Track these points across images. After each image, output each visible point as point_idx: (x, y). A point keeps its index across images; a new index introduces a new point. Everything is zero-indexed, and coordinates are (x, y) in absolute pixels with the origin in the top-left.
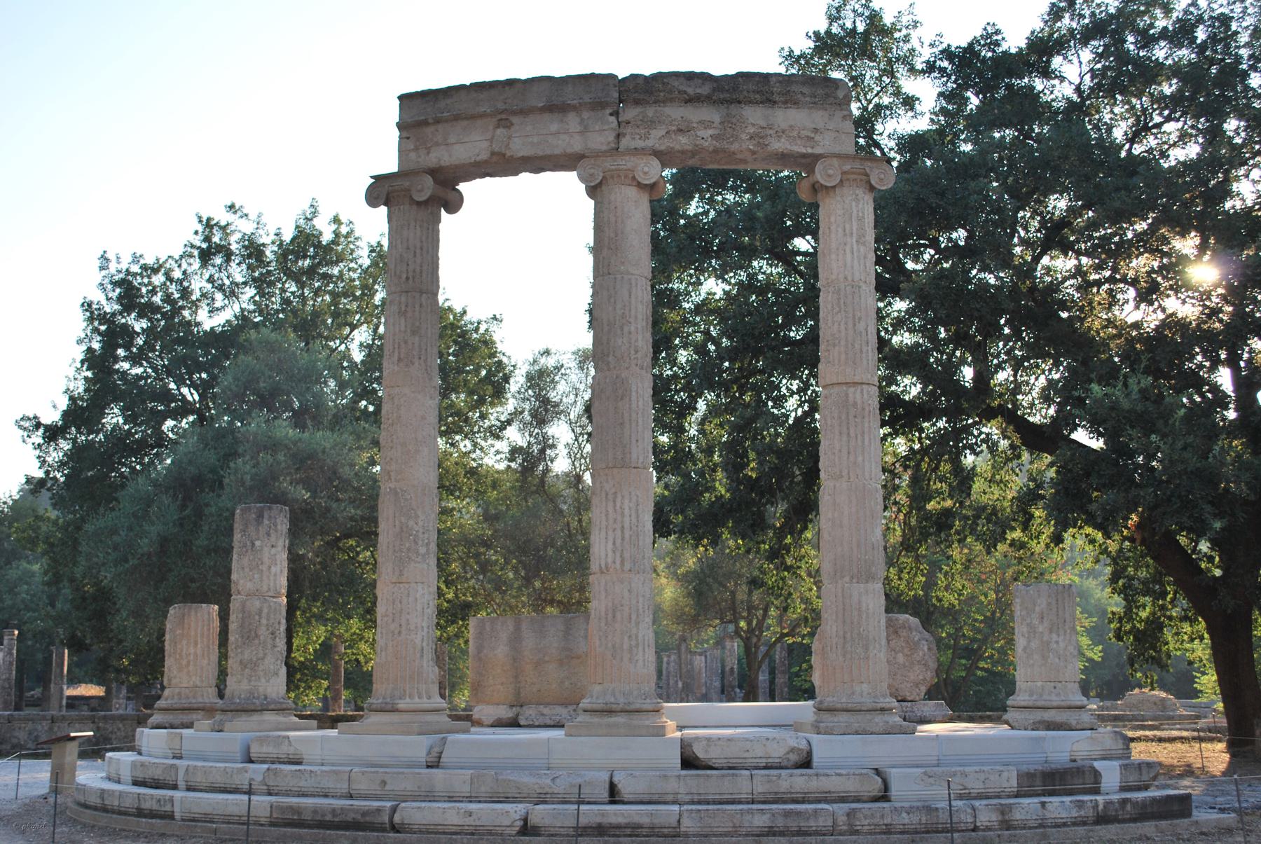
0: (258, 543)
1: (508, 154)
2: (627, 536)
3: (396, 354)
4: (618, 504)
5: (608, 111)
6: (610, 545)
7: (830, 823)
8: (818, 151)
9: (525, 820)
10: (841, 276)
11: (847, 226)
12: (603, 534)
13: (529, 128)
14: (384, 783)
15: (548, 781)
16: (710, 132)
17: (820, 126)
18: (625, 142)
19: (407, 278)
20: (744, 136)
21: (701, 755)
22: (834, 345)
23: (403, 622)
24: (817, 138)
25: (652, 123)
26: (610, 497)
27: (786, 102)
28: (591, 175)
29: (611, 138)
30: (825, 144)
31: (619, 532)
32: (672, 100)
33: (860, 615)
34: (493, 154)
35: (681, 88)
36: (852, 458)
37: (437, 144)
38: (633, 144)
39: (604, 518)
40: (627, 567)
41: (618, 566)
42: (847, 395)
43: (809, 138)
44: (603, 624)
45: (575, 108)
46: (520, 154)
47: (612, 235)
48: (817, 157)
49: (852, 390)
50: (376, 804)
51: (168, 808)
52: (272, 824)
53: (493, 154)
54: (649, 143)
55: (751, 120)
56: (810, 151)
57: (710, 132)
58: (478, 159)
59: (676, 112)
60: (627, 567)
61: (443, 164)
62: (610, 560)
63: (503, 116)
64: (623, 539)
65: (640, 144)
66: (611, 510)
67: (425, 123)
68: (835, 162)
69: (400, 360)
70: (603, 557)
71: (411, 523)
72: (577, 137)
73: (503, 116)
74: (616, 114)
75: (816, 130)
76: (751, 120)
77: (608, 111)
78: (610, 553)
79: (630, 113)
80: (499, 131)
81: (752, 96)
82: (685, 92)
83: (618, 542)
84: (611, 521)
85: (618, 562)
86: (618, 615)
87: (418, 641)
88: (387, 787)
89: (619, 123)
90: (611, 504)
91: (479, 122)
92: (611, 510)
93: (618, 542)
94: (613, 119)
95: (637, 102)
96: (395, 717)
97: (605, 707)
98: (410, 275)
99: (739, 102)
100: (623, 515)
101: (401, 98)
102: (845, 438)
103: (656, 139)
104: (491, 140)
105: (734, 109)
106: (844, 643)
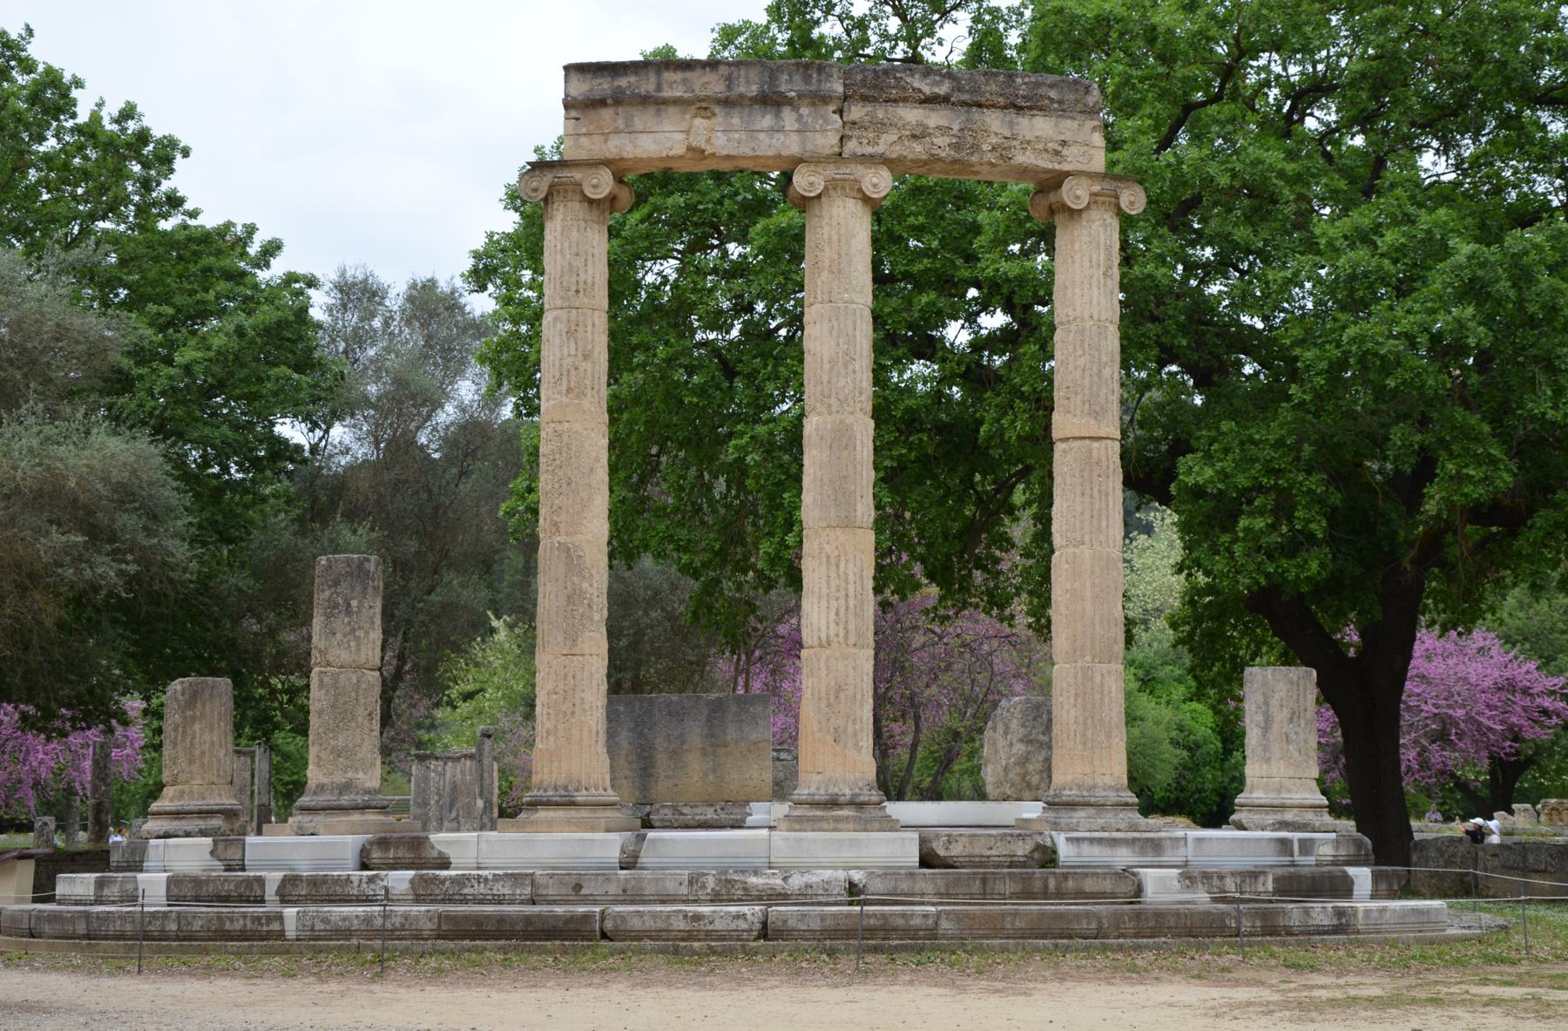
0: (354, 603)
1: (709, 150)
2: (851, 604)
3: (565, 382)
4: (842, 569)
5: (832, 108)
6: (832, 615)
7: (1094, 926)
8: (1066, 167)
9: (765, 924)
10: (1086, 315)
11: (1094, 257)
12: (824, 604)
13: (736, 121)
14: (578, 887)
15: (779, 881)
16: (947, 140)
17: (1067, 136)
18: (851, 146)
19: (577, 291)
20: (985, 147)
21: (942, 853)
22: (1076, 393)
23: (577, 701)
24: (1065, 152)
25: (881, 127)
26: (832, 560)
27: (1031, 108)
28: (811, 184)
29: (835, 140)
30: (1072, 160)
31: (842, 601)
32: (905, 100)
33: (1102, 699)
34: (690, 148)
35: (916, 85)
36: (1095, 522)
37: (617, 131)
38: (859, 151)
39: (824, 585)
40: (852, 640)
41: (841, 639)
42: (1090, 451)
43: (1057, 153)
44: (823, 705)
45: (790, 102)
46: (724, 153)
47: (835, 257)
48: (1068, 174)
49: (1096, 445)
50: (581, 909)
51: (275, 926)
52: (439, 937)
53: (690, 148)
54: (879, 149)
55: (994, 128)
56: (1057, 167)
57: (947, 140)
58: (672, 153)
59: (911, 115)
60: (852, 640)
61: (625, 155)
62: (832, 633)
64: (847, 608)
65: (869, 150)
66: (833, 575)
67: (601, 103)
68: (1084, 181)
69: (569, 390)
70: (823, 628)
71: (585, 585)
72: (795, 137)
74: (840, 112)
75: (1064, 143)
76: (994, 128)
77: (832, 108)
78: (832, 625)
79: (856, 112)
81: (995, 98)
82: (920, 91)
83: (842, 612)
84: (833, 588)
85: (842, 633)
86: (842, 695)
87: (593, 723)
88: (583, 892)
89: (844, 123)
90: (833, 568)
91: (672, 110)
92: (833, 575)
93: (842, 612)
94: (836, 117)
95: (865, 99)
96: (572, 813)
97: (809, 799)
98: (581, 287)
99: (980, 106)
100: (846, 580)
101: (567, 68)
102: (1087, 497)
103: (886, 144)
104: (687, 132)
105: (975, 113)
106: (1086, 729)
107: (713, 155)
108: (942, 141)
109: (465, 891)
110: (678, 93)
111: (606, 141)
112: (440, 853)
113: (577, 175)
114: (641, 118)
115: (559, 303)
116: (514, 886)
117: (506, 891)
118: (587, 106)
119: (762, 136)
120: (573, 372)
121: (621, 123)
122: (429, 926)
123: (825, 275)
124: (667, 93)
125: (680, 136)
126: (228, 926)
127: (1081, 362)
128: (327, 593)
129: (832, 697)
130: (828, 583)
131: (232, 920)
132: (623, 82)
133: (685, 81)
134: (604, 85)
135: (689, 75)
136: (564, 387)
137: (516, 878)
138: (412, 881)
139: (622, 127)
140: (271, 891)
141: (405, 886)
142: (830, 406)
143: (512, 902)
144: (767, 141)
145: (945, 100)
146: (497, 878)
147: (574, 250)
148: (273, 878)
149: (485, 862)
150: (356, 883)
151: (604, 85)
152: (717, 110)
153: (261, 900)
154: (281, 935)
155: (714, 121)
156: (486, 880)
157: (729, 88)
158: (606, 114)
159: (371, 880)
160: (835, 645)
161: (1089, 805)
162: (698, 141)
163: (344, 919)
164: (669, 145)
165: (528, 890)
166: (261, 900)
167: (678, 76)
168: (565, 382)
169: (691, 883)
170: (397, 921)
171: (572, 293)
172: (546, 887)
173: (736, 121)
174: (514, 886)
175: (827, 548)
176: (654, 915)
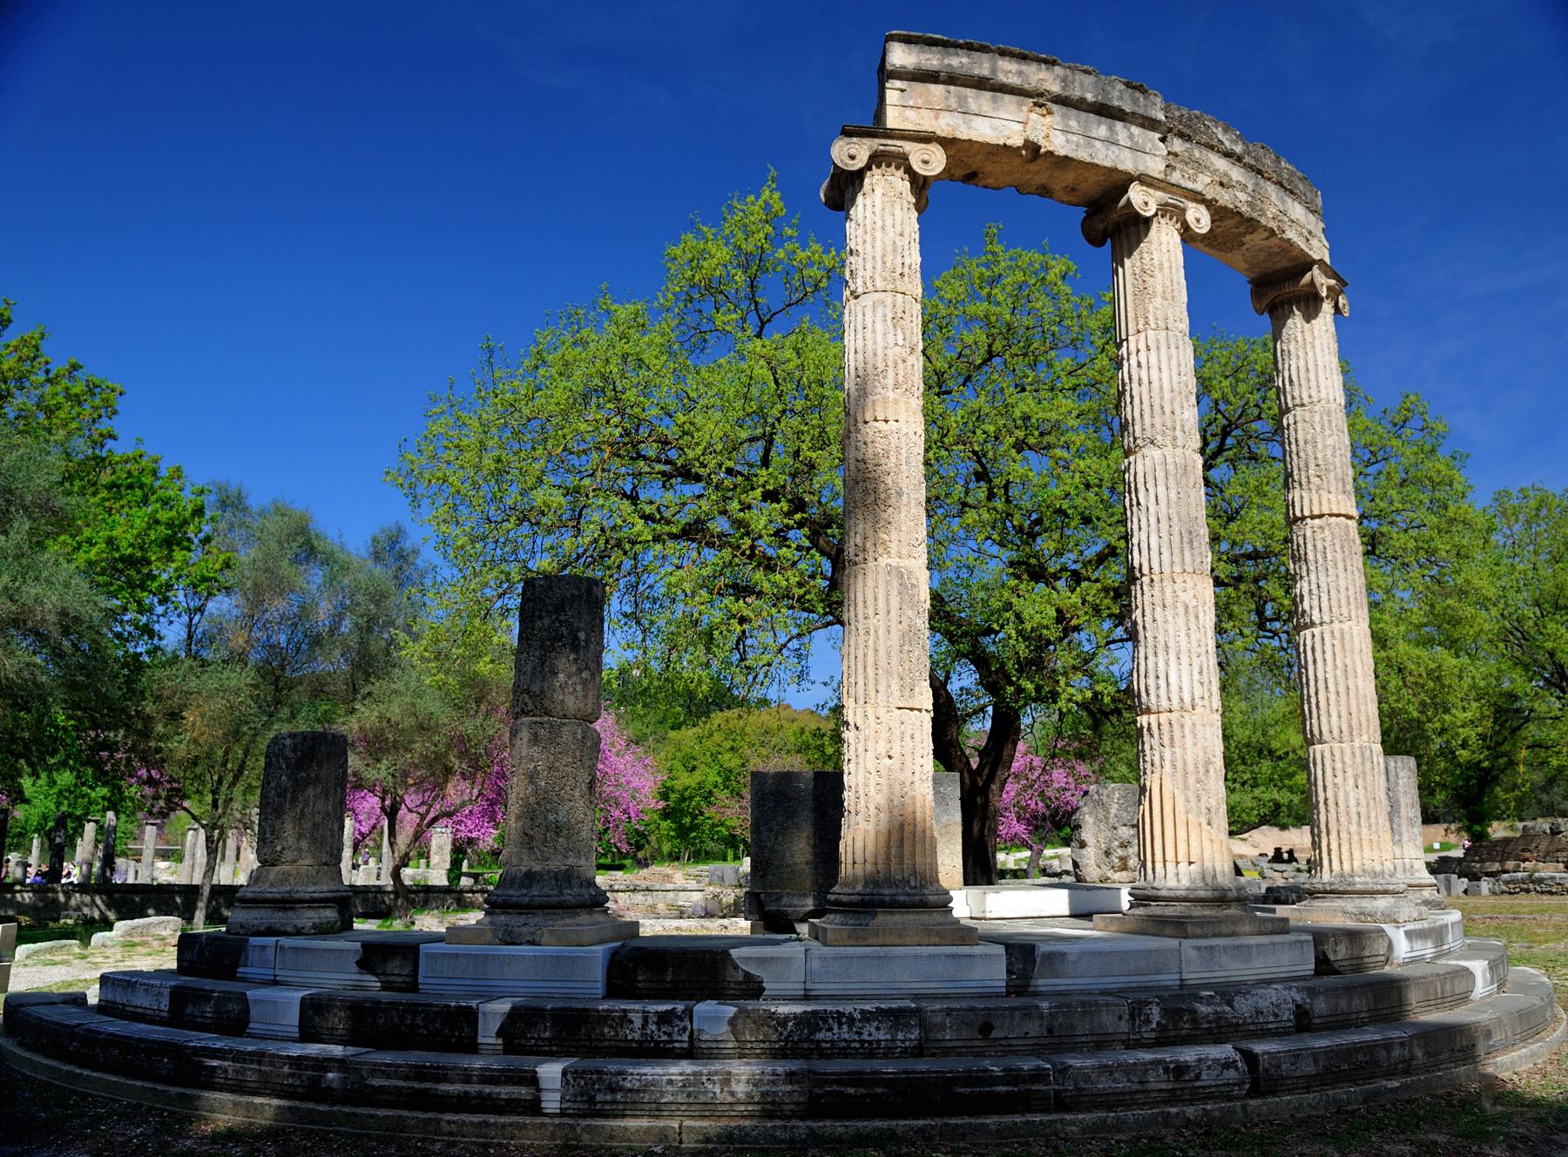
0: (582, 635)
14: (986, 1029)
25: (1199, 166)
31: (1203, 658)
34: (1027, 141)
39: (1183, 638)
47: (1168, 283)
54: (1198, 187)
58: (1009, 143)
59: (1221, 164)
61: (959, 136)
63: (1041, 101)
65: (1190, 185)
69: (896, 386)
73: (1041, 101)
79: (1178, 145)
80: (1033, 116)
84: (1194, 644)
88: (994, 1034)
90: (1192, 619)
107: (1050, 153)
108: (1242, 196)
109: (820, 1036)
110: (1013, 80)
111: (936, 118)
112: (747, 974)
113: (907, 146)
114: (979, 100)
115: (880, 285)
116: (895, 1027)
117: (882, 1035)
118: (914, 79)
119: (1098, 144)
120: (901, 366)
121: (953, 102)
123: (1158, 301)
124: (1002, 78)
125: (1019, 127)
127: (1330, 441)
128: (547, 621)
129: (1202, 770)
130: (1188, 635)
133: (1020, 73)
135: (1024, 67)
137: (896, 1017)
139: (954, 106)
142: (1175, 438)
143: (888, 1054)
144: (1103, 150)
145: (1239, 159)
146: (867, 1017)
147: (898, 230)
149: (819, 988)
150: (638, 1023)
152: (1054, 107)
153: (472, 1047)
155: (1049, 119)
156: (851, 1020)
157: (1064, 88)
158: (937, 90)
159: (664, 1018)
160: (1199, 710)
161: (1386, 892)
162: (1037, 137)
164: (1006, 133)
165: (915, 1034)
166: (472, 1047)
168: (891, 374)
169: (1132, 1016)
171: (897, 275)
172: (942, 1027)
173: (1073, 124)
174: (895, 1027)
175: (1183, 596)
176: (1128, 1069)
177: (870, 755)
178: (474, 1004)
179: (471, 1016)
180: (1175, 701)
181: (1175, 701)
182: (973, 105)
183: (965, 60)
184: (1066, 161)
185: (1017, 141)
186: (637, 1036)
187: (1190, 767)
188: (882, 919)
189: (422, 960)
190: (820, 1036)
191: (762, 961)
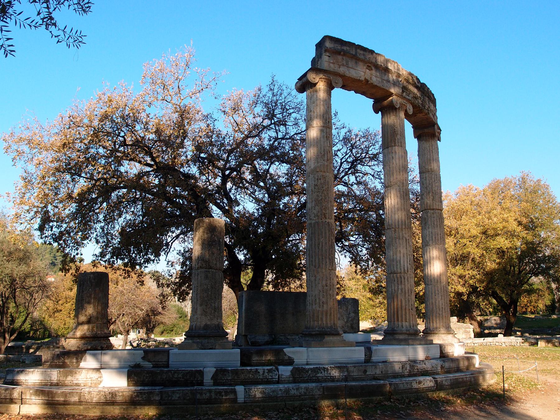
37: (343, 65)
58: (360, 79)
88: (368, 373)
109: (318, 375)
111: (339, 67)
112: (289, 357)
118: (333, 53)
122: (319, 393)
126: (198, 396)
131: (201, 394)
132: (345, 48)
133: (364, 55)
134: (339, 47)
135: (365, 53)
136: (326, 158)
138: (292, 371)
139: (345, 64)
140: (208, 378)
141: (289, 374)
148: (209, 372)
149: (311, 361)
150: (261, 373)
151: (339, 47)
153: (201, 383)
154: (235, 400)
155: (371, 71)
158: (340, 57)
159: (270, 371)
163: (273, 391)
167: (362, 52)
168: (326, 156)
170: (303, 391)
172: (353, 372)
173: (378, 74)
177: (320, 285)
178: (202, 369)
179: (201, 373)
180: (402, 270)
181: (402, 270)
182: (350, 65)
183: (348, 48)
184: (375, 87)
185: (362, 78)
186: (261, 377)
187: (407, 291)
188: (328, 339)
189: (171, 356)
190: (318, 375)
191: (293, 353)
